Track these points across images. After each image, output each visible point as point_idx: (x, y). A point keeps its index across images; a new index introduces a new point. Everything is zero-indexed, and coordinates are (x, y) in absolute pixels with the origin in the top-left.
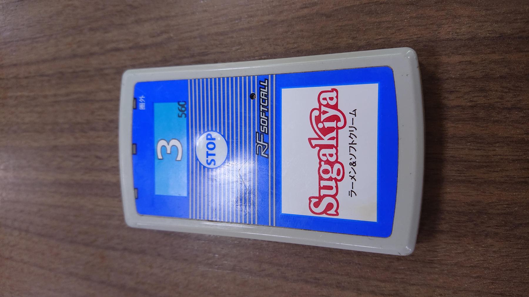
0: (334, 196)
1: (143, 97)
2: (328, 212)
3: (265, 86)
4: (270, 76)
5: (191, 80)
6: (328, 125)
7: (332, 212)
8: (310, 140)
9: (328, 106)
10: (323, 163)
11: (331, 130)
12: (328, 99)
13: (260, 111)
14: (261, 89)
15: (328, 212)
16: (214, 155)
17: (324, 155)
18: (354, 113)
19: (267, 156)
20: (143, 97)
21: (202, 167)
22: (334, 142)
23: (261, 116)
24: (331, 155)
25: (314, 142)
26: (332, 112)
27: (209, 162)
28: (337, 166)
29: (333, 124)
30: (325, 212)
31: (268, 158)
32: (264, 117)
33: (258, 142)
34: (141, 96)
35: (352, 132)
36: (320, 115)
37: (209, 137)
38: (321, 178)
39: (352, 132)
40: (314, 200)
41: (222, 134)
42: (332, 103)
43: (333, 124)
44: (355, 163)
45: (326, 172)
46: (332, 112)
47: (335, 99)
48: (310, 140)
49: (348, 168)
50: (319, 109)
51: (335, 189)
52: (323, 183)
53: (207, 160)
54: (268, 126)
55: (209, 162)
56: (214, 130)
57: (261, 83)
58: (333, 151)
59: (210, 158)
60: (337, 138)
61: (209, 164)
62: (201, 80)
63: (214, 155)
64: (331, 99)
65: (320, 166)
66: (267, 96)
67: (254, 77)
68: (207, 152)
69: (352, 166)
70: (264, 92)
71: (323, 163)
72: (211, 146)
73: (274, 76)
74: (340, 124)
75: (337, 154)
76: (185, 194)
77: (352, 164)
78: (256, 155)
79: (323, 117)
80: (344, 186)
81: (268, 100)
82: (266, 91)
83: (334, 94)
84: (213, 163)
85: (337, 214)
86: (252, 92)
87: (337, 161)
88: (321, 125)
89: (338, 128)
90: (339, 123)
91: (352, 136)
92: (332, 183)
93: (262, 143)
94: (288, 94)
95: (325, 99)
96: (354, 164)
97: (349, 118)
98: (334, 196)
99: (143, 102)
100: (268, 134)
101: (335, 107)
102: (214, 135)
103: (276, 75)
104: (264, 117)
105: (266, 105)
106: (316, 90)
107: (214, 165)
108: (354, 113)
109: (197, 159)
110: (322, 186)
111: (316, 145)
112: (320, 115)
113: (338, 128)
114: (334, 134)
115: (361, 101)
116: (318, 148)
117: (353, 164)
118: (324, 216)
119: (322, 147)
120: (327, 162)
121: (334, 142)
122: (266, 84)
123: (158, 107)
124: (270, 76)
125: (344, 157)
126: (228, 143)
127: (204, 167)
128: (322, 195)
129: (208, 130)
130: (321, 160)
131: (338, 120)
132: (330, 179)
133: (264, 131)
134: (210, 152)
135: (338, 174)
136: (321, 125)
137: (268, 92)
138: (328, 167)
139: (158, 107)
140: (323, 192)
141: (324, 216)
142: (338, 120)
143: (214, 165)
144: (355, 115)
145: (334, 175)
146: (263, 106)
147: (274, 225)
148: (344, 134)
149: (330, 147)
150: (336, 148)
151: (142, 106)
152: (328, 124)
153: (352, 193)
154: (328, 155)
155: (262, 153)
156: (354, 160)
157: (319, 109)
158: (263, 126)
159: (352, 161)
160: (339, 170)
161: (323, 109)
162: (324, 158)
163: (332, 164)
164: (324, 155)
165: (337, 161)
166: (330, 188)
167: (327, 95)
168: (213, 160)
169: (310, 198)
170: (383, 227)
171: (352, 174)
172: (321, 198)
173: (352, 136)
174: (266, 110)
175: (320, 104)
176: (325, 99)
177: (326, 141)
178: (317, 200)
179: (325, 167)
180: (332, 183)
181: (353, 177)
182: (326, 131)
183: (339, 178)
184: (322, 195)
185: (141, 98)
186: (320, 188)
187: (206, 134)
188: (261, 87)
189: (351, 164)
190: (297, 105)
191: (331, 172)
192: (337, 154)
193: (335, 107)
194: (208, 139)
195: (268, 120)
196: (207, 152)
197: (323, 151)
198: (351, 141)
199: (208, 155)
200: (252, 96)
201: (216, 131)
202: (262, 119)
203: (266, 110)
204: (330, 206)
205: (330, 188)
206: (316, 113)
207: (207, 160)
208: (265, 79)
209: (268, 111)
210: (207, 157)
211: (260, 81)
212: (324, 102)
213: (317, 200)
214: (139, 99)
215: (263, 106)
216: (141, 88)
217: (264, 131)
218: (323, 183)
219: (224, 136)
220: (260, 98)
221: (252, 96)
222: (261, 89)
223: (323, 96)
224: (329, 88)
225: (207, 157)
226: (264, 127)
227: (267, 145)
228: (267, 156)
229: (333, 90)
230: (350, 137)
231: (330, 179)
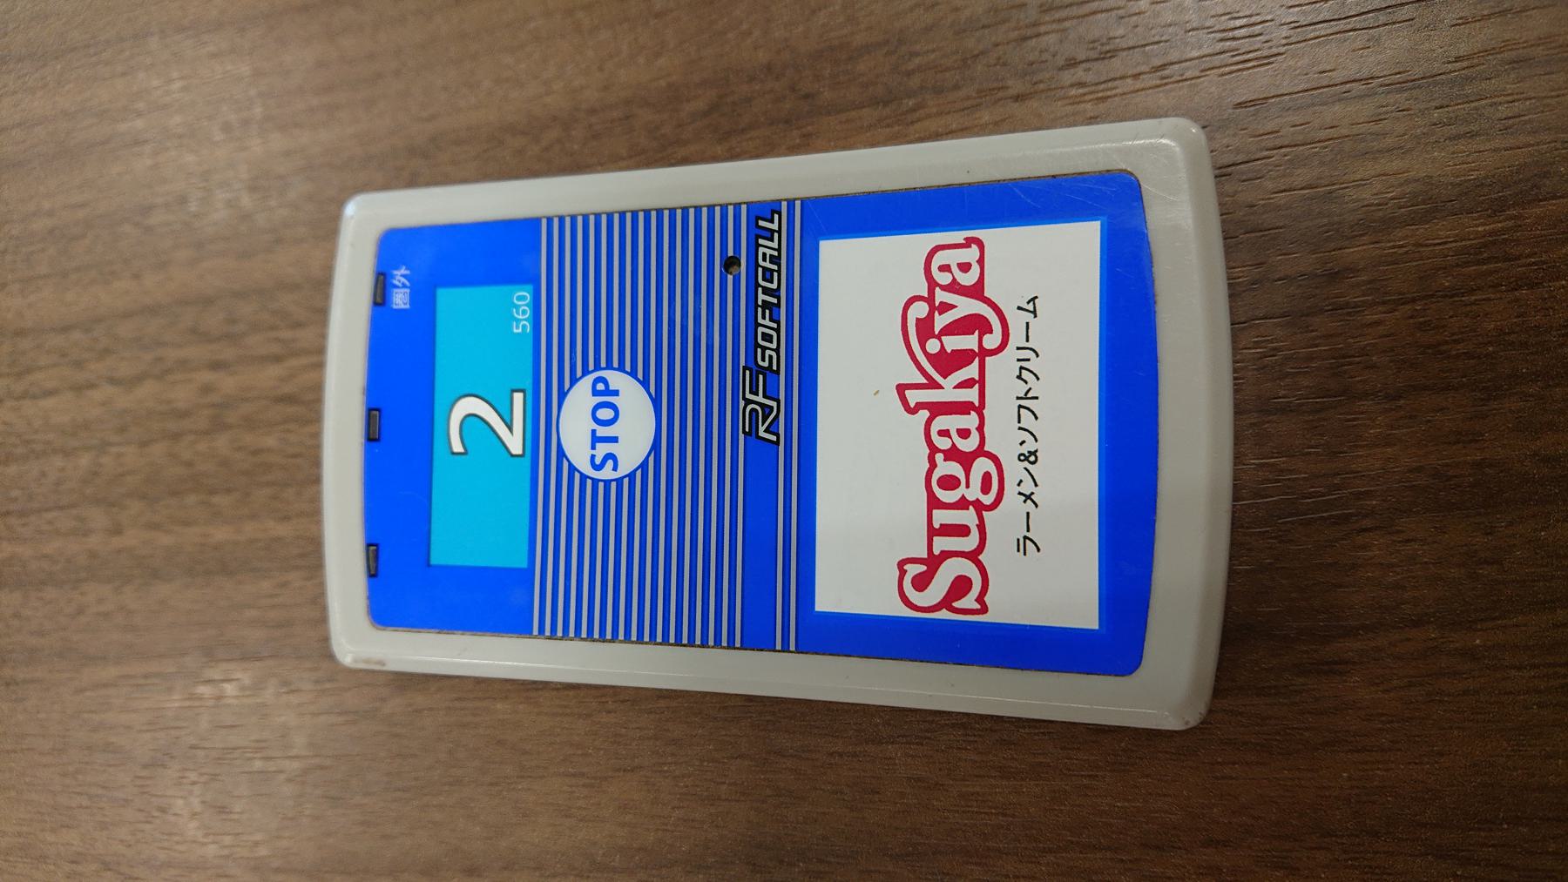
0: (973, 556)
1: (403, 271)
2: (956, 604)
3: (773, 231)
4: (784, 204)
5: (550, 220)
6: (954, 343)
7: (969, 602)
8: (901, 389)
9: (954, 287)
10: (939, 457)
11: (963, 358)
12: (955, 269)
13: (757, 306)
14: (761, 241)
15: (956, 604)
16: (614, 440)
17: (944, 433)
18: (1031, 307)
19: (774, 438)
20: (403, 271)
21: (577, 475)
22: (972, 395)
23: (760, 321)
24: (964, 433)
25: (914, 397)
27: (598, 461)
28: (982, 465)
29: (969, 342)
30: (946, 603)
31: (777, 443)
32: (767, 322)
33: (748, 396)
34: (397, 268)
35: (1024, 364)
36: (930, 316)
37: (600, 387)
38: (934, 503)
39: (1024, 364)
40: (913, 570)
41: (640, 376)
42: (968, 279)
43: (969, 342)
44: (1034, 453)
45: (949, 483)
46: (966, 306)
47: (976, 269)
48: (901, 389)
49: (1014, 470)
50: (930, 299)
51: (975, 533)
52: (942, 517)
53: (593, 457)
54: (777, 351)
55: (598, 461)
56: (616, 365)
57: (761, 223)
58: (970, 421)
59: (602, 449)
60: (982, 381)
61: (598, 468)
62: (580, 219)
63: (614, 440)
64: (964, 267)
65: (933, 465)
66: (775, 260)
67: (737, 206)
68: (594, 432)
69: (1026, 464)
70: (767, 248)
71: (939, 457)
72: (605, 414)
73: (798, 203)
74: (991, 341)
75: (980, 429)
76: (522, 563)
77: (1027, 459)
78: (741, 436)
79: (940, 321)
80: (1004, 523)
81: (779, 272)
82: (775, 245)
83: (972, 254)
84: (610, 463)
85: (984, 609)
86: (731, 253)
87: (980, 451)
88: (933, 346)
89: (984, 353)
90: (986, 337)
91: (1025, 374)
92: (968, 517)
93: (760, 399)
94: (840, 259)
95: (945, 268)
96: (1032, 459)
97: (1016, 321)
98: (973, 556)
99: (404, 286)
100: (778, 372)
101: (976, 291)
102: (616, 379)
103: (803, 201)
104: (767, 322)
105: (774, 286)
106: (917, 244)
107: (615, 469)
108: (1031, 307)
109: (561, 454)
110: (937, 526)
111: (920, 406)
112: (930, 316)
113: (984, 353)
114: (972, 371)
115: (1049, 274)
116: (924, 414)
117: (1030, 457)
118: (944, 614)
119: (937, 409)
120: (952, 454)
121: (972, 395)
122: (775, 226)
123: (447, 298)
124: (784, 204)
125: (1003, 438)
126: (656, 402)
127: (584, 477)
128: (936, 552)
129: (597, 367)
131: (985, 328)
132: (962, 504)
133: (766, 364)
134: (602, 432)
135: (986, 489)
136: (933, 346)
137: (779, 250)
138: (955, 469)
139: (447, 298)
140: (941, 544)
141: (944, 614)
142: (985, 328)
143: (615, 469)
144: (1034, 312)
145: (974, 493)
146: (766, 291)
147: (792, 648)
148: (1000, 370)
149: (963, 408)
150: (980, 410)
151: (400, 299)
152: (953, 343)
153: (1025, 543)
154: (954, 434)
155: (762, 429)
156: (1030, 446)
157: (930, 299)
158: (764, 349)
159: (1025, 450)
160: (987, 478)
161: (941, 296)
162: (943, 443)
163: (966, 460)
164: (944, 433)
165: (980, 451)
166: (963, 531)
167: (952, 257)
168: (610, 456)
169: (901, 565)
170: (1115, 643)
171: (1027, 487)
172: (934, 562)
173: (1025, 374)
174: (775, 301)
175: (932, 284)
176: (945, 268)
177: (949, 391)
178: (923, 568)
180: (968, 517)
181: (1028, 497)
182: (948, 362)
183: (988, 500)
184: (936, 552)
185: (399, 275)
186: (932, 532)
187: (590, 379)
188: (757, 234)
189: (1023, 458)
190: (865, 291)
191: (962, 481)
192: (980, 429)
193: (976, 291)
194: (595, 393)
195: (778, 331)
196: (594, 432)
197: (942, 422)
198: (1021, 389)
199: (595, 440)
200: (730, 263)
201: (621, 368)
202: (760, 330)
203: (775, 301)
204: (961, 586)
205: (963, 531)
206: (920, 310)
207: (593, 457)
208: (773, 212)
209: (778, 305)
210: (593, 448)
211: (758, 218)
212: (944, 279)
213: (923, 568)
214: (393, 277)
215: (766, 291)
216: (395, 246)
217: (766, 364)
219: (645, 383)
220: (757, 265)
221: (730, 263)
222: (761, 241)
223: (940, 259)
224: (958, 236)
225: (593, 448)
226: (768, 352)
227: (774, 404)
228: (774, 438)
229: (969, 242)
230: (1019, 377)
231: (962, 504)
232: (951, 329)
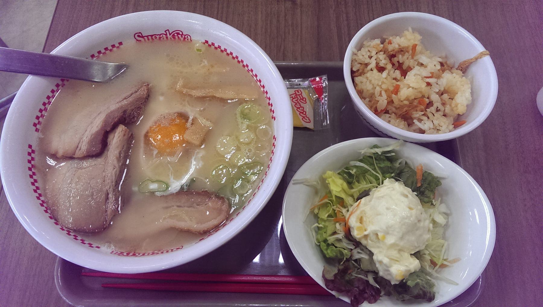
6: (177, 37)
9: (185, 38)
25: (167, 32)
26: (182, 39)
38: (152, 36)
45: (156, 38)
52: (150, 37)
79: (180, 36)
88: (176, 35)
119: (166, 35)
120: (160, 38)
130: (160, 35)
136: (176, 35)
138: (158, 38)
172: (143, 37)
179: (158, 37)
186: (147, 36)
206: (181, 33)
212: (186, 37)
218: (150, 37)
232: (179, 38)
